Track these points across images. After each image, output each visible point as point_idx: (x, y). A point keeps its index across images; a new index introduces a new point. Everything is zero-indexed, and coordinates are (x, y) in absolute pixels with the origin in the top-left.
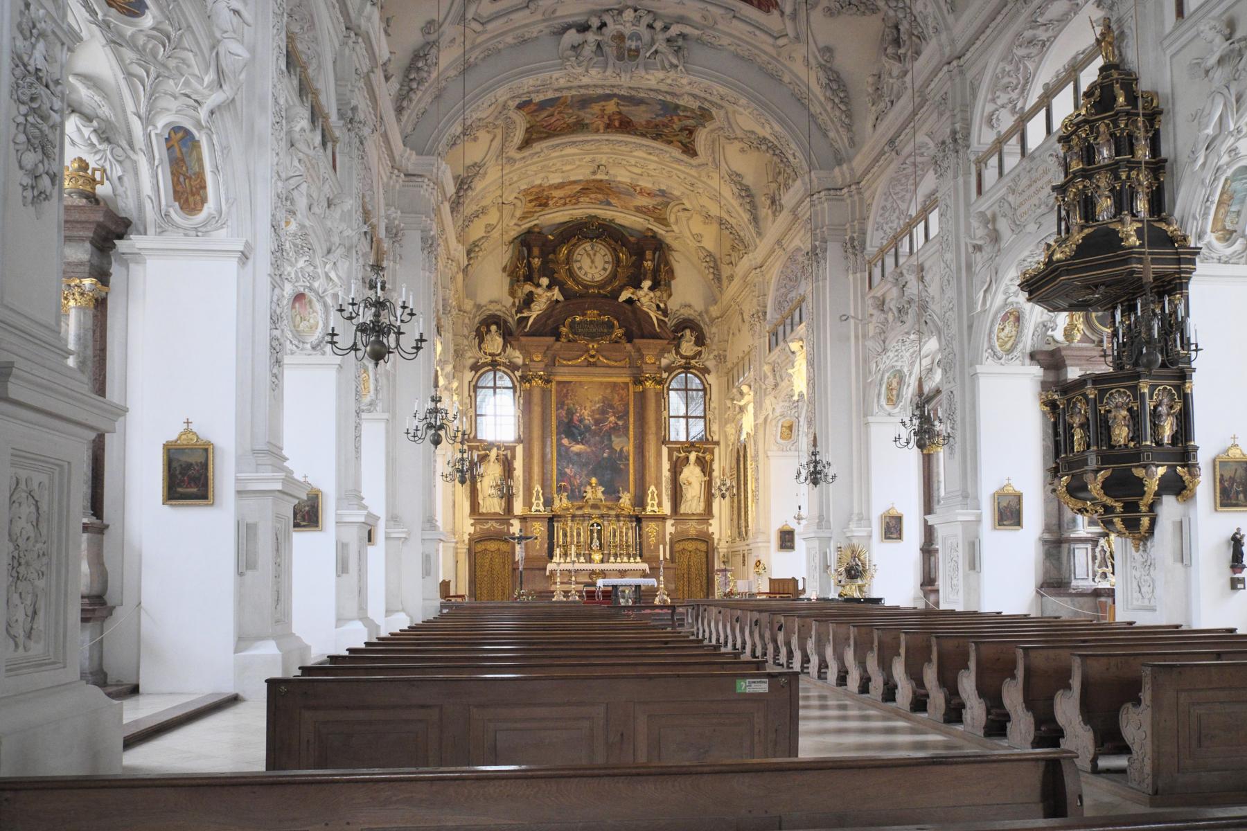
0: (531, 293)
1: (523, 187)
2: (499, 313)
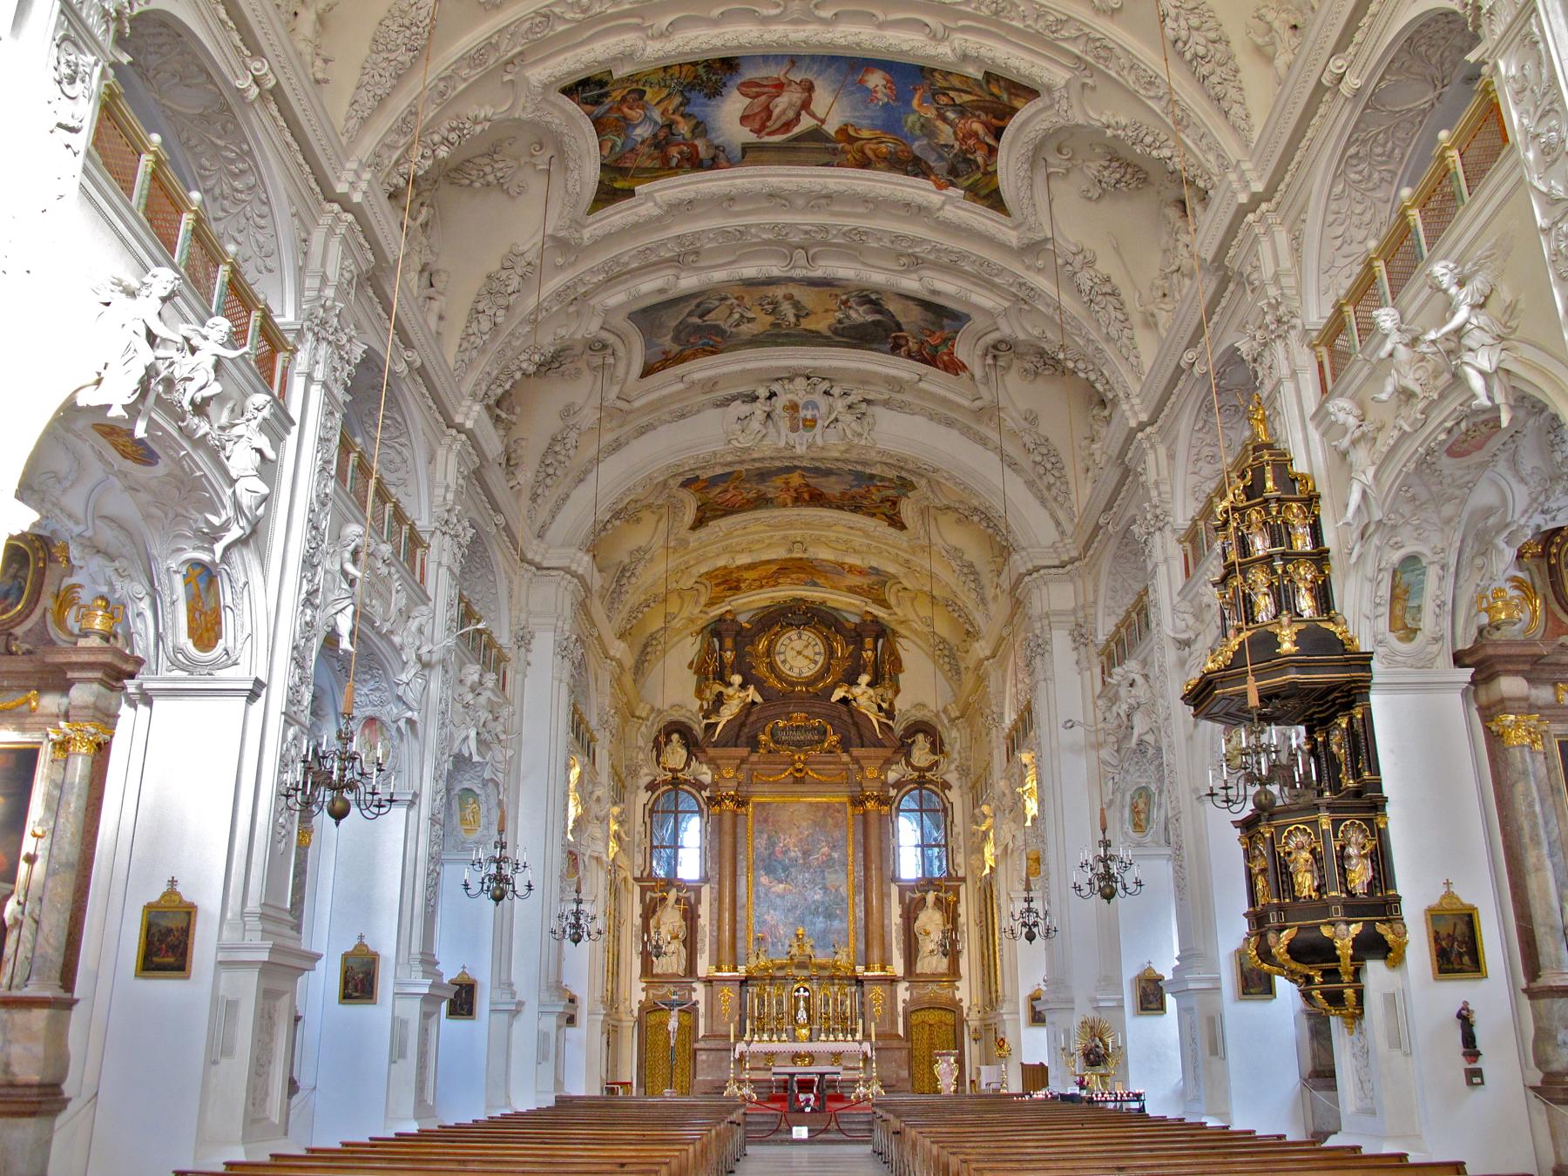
0: (721, 693)
1: (704, 569)
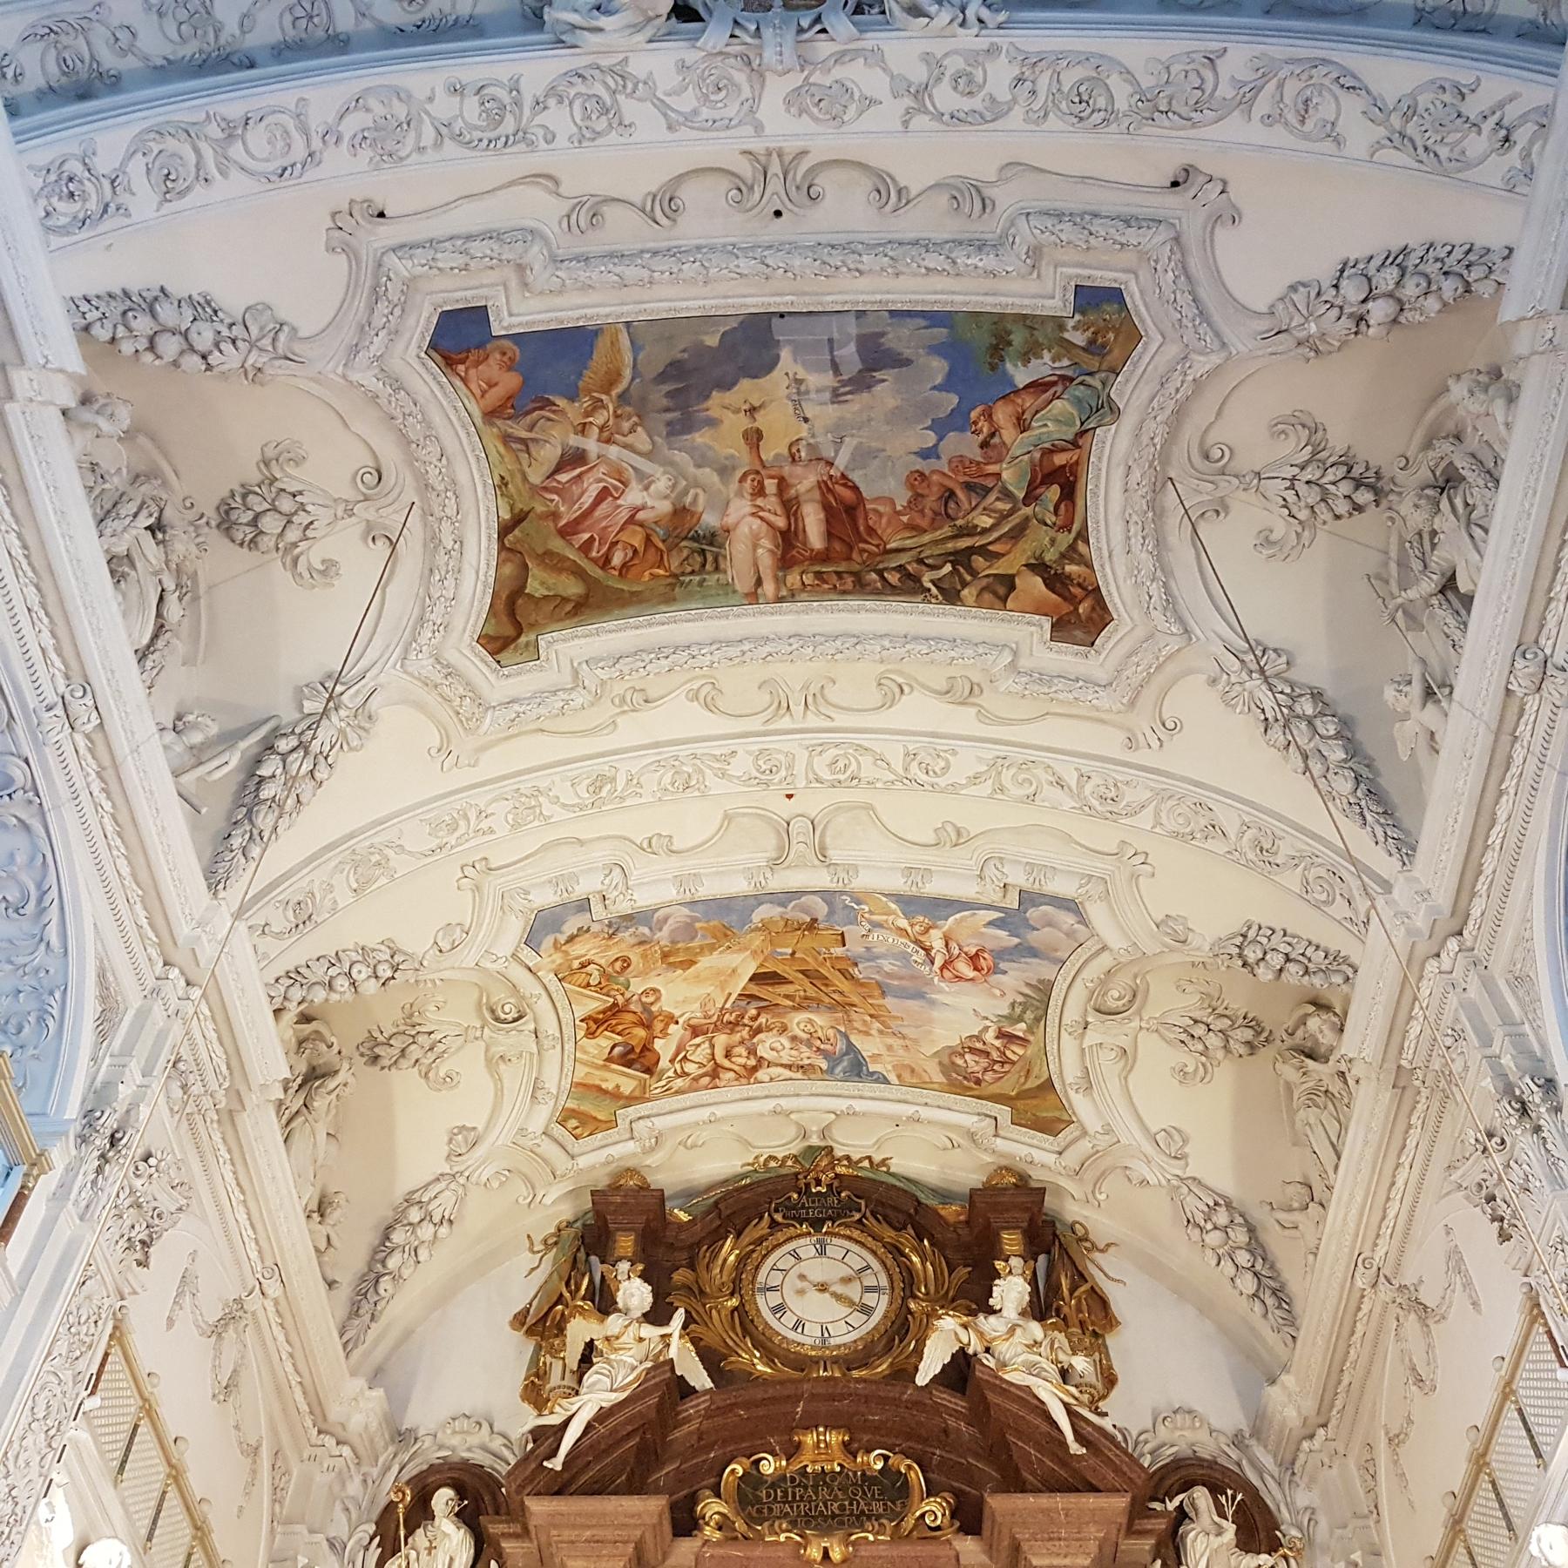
2: (479, 1457)
